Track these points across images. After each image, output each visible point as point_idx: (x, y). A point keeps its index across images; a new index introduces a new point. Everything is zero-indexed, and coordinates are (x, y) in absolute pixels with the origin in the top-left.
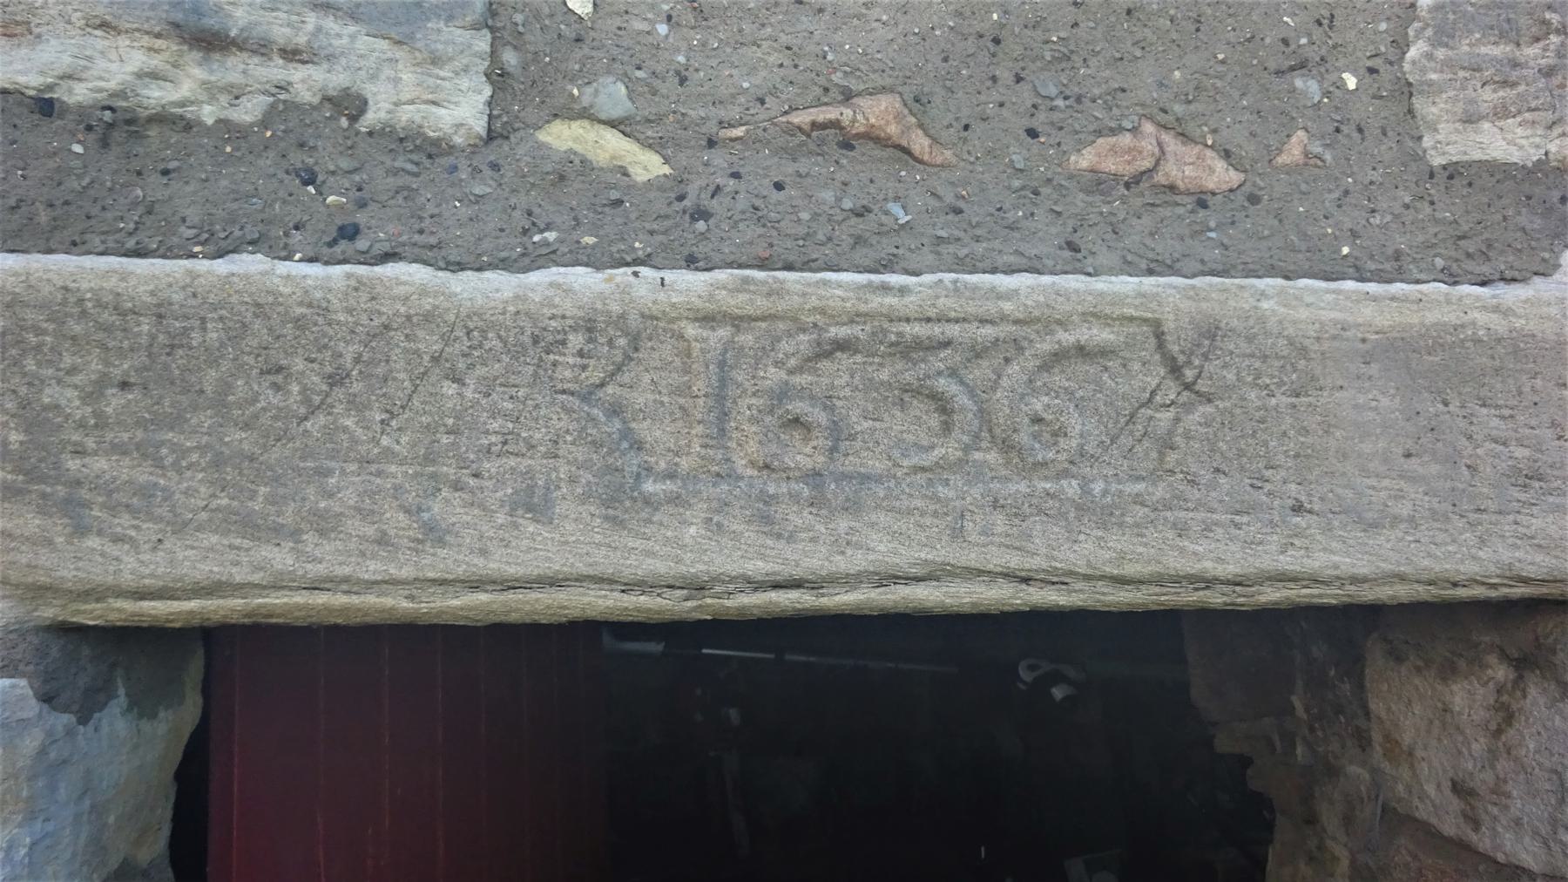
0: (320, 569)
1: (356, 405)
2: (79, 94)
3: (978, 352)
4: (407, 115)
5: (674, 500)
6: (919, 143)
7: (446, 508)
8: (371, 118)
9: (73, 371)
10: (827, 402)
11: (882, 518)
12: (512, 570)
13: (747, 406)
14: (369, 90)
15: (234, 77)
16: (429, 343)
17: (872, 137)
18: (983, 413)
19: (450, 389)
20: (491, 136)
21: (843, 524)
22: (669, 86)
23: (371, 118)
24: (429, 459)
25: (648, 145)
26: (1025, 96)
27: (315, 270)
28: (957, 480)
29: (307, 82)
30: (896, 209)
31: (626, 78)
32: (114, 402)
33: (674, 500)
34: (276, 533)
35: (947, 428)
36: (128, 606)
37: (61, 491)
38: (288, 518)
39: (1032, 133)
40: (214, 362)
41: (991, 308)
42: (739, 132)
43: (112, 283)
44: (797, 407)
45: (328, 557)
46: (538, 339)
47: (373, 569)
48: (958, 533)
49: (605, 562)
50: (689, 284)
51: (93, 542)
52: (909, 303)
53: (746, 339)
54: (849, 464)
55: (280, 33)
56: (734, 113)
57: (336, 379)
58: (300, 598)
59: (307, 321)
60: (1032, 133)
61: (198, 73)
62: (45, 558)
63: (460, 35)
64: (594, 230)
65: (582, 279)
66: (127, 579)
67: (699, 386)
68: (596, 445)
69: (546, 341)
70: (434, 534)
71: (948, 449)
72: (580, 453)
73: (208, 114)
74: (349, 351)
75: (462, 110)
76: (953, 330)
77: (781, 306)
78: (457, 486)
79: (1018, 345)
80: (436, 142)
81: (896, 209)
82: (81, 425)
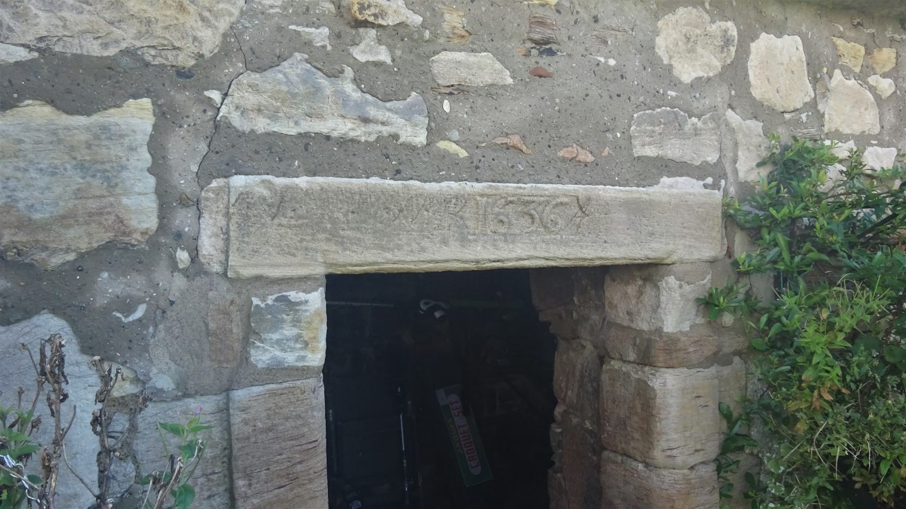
0: (398, 258)
1: (406, 217)
2: (335, 134)
3: (540, 204)
4: (410, 139)
5: (475, 240)
6: (524, 148)
7: (425, 243)
8: (401, 140)
9: (341, 209)
10: (507, 216)
11: (519, 245)
12: (439, 258)
13: (491, 217)
14: (400, 132)
15: (370, 130)
16: (421, 202)
17: (514, 147)
18: (541, 219)
19: (426, 213)
20: (428, 144)
21: (511, 246)
22: (467, 132)
23: (401, 140)
24: (422, 231)
25: (462, 148)
26: (547, 136)
27: (392, 182)
28: (535, 235)
29: (385, 130)
30: (520, 166)
31: (458, 130)
32: (351, 216)
33: (475, 240)
34: (389, 250)
35: (533, 222)
36: (350, 268)
37: (340, 240)
38: (391, 246)
39: (549, 146)
40: (373, 206)
41: (543, 193)
42: (484, 145)
43: (349, 186)
44: (502, 217)
45: (399, 255)
46: (446, 200)
47: (409, 258)
48: (535, 248)
49: (460, 256)
50: (478, 186)
51: (348, 252)
52: (525, 192)
53: (490, 200)
54: (512, 231)
55: (380, 118)
56: (481, 139)
57: (401, 211)
58: (391, 266)
59: (393, 196)
60: (549, 146)
61: (363, 129)
62: (336, 256)
63: (422, 119)
64: (453, 171)
65: (453, 184)
66: (354, 262)
67: (481, 212)
68: (458, 227)
69: (447, 201)
70: (423, 250)
71: (533, 228)
72: (455, 229)
73: (363, 139)
74: (404, 203)
75: (421, 138)
76: (535, 199)
77: (498, 192)
78: (428, 238)
79: (548, 202)
80: (414, 147)
81: (520, 166)
82: (344, 223)
